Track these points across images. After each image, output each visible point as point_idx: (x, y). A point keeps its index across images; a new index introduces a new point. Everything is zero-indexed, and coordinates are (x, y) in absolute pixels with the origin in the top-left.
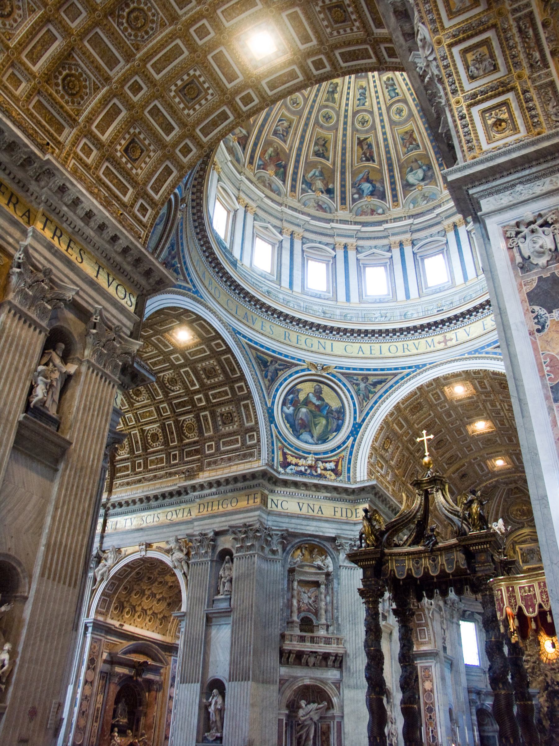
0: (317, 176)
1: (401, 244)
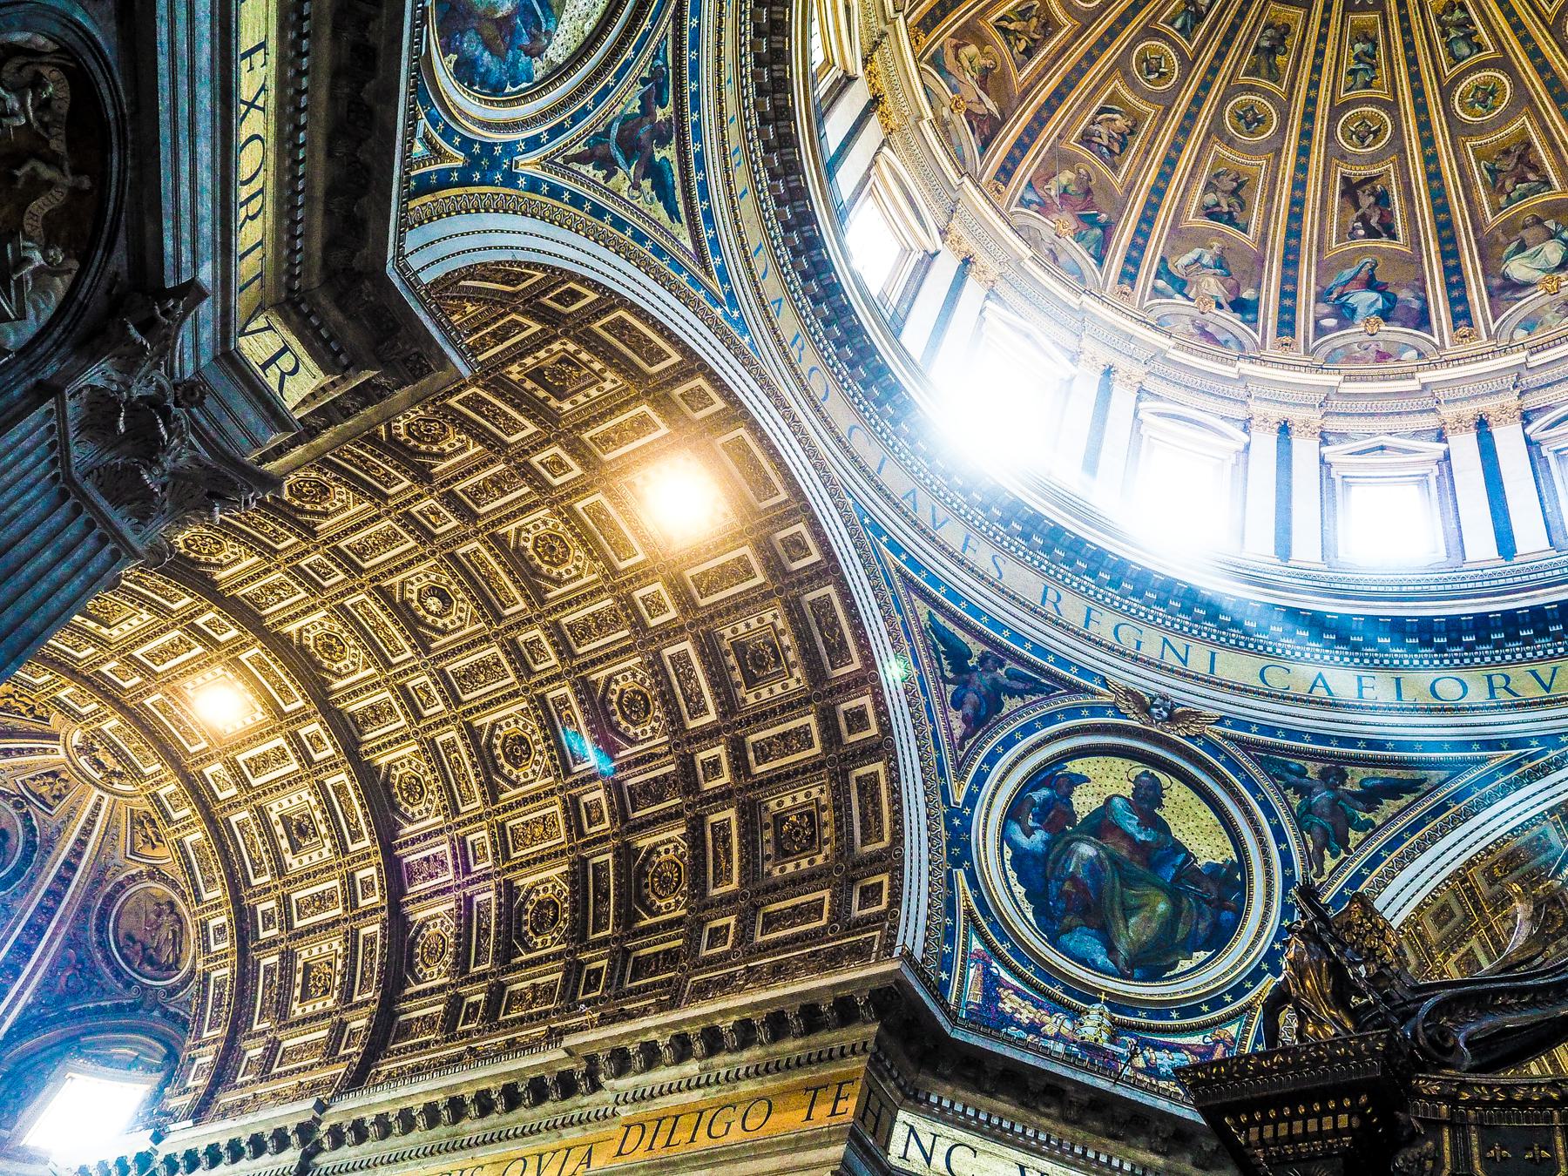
0: (1204, 266)
1: (1482, 425)
